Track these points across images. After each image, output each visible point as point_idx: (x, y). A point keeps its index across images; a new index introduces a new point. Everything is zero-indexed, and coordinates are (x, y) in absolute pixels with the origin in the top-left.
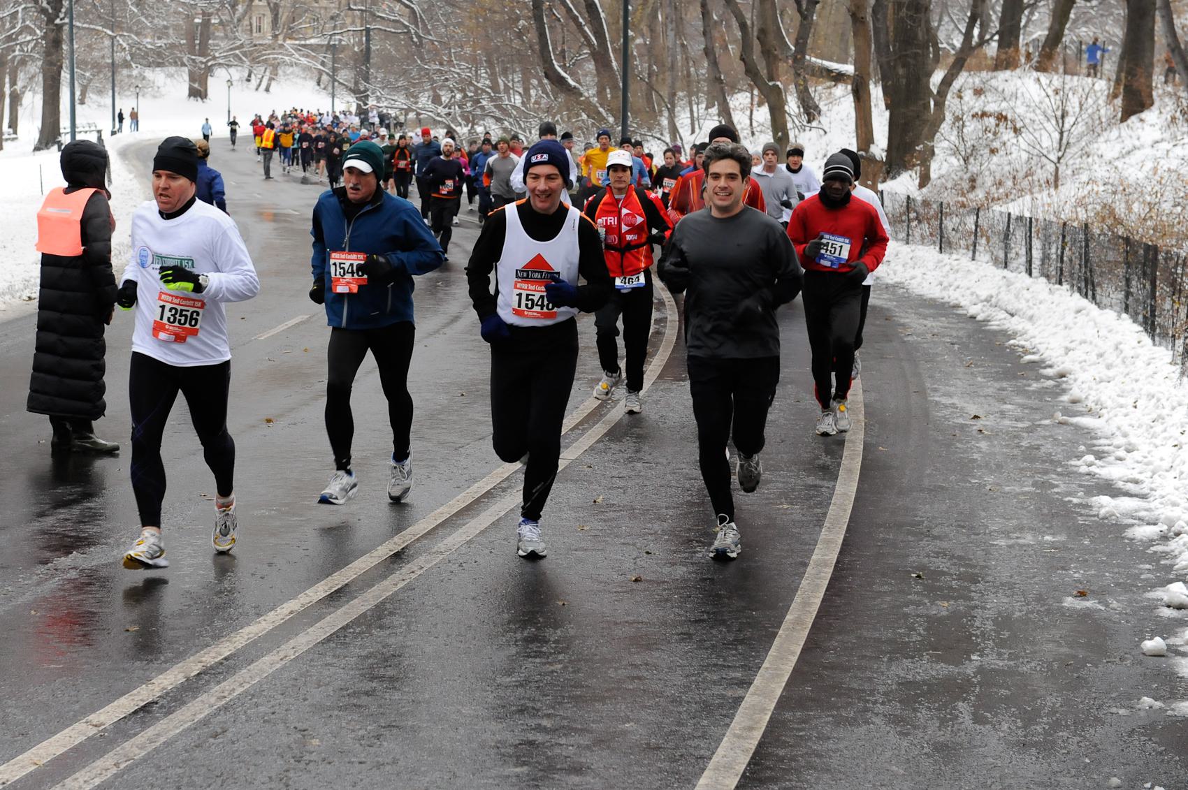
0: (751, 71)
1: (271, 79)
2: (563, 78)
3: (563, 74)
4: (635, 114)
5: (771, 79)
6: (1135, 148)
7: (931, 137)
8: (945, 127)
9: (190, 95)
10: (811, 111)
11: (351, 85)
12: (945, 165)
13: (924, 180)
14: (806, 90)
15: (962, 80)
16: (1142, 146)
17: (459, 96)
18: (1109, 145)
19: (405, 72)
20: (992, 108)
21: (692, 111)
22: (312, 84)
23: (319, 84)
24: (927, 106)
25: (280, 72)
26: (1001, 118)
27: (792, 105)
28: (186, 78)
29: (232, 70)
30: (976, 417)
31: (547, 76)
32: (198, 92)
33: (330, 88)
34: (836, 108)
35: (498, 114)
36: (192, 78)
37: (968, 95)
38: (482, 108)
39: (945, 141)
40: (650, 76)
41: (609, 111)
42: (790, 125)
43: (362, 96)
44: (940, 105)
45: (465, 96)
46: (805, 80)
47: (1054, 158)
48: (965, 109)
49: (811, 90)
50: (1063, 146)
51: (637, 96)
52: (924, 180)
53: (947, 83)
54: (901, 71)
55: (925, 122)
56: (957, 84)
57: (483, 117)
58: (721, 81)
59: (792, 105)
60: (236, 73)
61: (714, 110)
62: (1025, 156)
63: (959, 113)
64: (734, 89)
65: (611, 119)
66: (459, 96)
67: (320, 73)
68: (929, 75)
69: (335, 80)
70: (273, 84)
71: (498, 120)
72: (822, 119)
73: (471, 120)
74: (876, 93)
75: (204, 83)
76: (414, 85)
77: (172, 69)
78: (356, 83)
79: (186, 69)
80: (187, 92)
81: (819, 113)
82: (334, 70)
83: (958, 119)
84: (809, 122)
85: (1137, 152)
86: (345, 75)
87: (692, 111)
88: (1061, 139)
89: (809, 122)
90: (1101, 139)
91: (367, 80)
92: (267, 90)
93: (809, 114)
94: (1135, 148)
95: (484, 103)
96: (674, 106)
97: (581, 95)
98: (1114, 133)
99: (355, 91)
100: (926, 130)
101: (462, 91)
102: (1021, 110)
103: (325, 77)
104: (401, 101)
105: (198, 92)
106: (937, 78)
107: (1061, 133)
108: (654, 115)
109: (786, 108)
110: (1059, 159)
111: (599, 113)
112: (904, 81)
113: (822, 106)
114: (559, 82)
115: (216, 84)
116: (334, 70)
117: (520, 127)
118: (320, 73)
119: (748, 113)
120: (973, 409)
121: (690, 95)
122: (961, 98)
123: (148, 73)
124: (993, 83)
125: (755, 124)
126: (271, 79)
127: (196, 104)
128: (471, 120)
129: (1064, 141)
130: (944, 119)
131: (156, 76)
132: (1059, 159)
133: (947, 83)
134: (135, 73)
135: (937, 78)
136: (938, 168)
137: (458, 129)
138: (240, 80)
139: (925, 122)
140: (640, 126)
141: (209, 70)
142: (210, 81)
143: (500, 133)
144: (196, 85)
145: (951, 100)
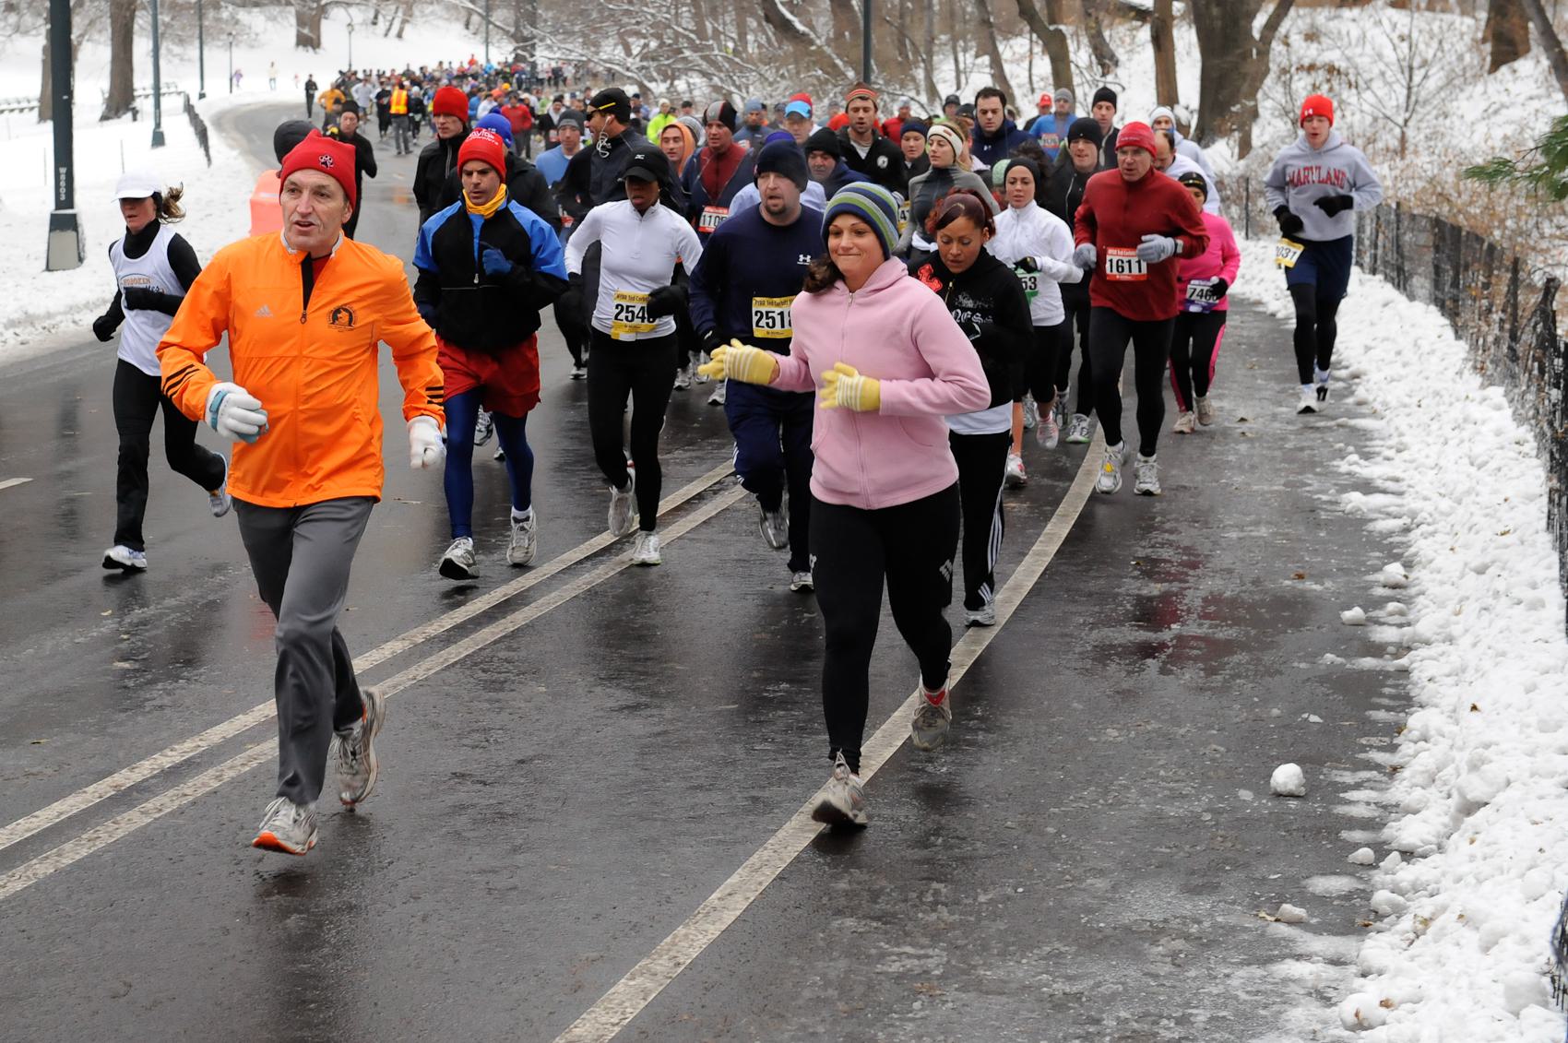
0: (1027, 13)
1: (404, 22)
2: (789, 22)
3: (789, 16)
4: (882, 67)
5: (1053, 21)
6: (1503, 106)
7: (1253, 95)
8: (1269, 81)
9: (298, 44)
10: (1105, 59)
11: (512, 30)
12: (1270, 129)
13: (1245, 147)
14: (1100, 34)
15: (1294, 23)
16: (1513, 104)
17: (653, 44)
18: (1470, 104)
19: (583, 13)
20: (1333, 56)
21: (956, 61)
22: (459, 26)
23: (467, 26)
24: (1246, 56)
25: (416, 12)
26: (1332, 69)
27: (1080, 55)
28: (293, 20)
29: (353, 11)
30: (1242, 420)
31: (768, 19)
32: (308, 40)
33: (483, 29)
34: (1136, 57)
35: (705, 66)
36: (301, 22)
37: (1296, 39)
38: (685, 59)
39: (1270, 99)
40: (902, 16)
41: (848, 63)
42: (1076, 80)
43: (525, 43)
44: (1264, 53)
45: (662, 44)
46: (1097, 21)
47: (1401, 121)
48: (1294, 59)
49: (1106, 34)
50: (1411, 103)
51: (883, 40)
52: (1245, 147)
53: (1272, 26)
54: (1215, 11)
55: (1244, 76)
56: (1282, 30)
57: (686, 71)
58: (990, 25)
59: (1080, 55)
60: (359, 15)
61: (986, 59)
62: (1369, 119)
63: (1285, 63)
64: (1010, 33)
65: (851, 74)
66: (653, 44)
67: (470, 12)
68: (1252, 16)
69: (489, 22)
70: (408, 27)
71: (704, 74)
72: (1119, 71)
73: (670, 76)
74: (1186, 39)
75: (316, 27)
76: (595, 30)
77: (275, 10)
78: (517, 27)
79: (292, 10)
80: (294, 40)
81: (1116, 64)
82: (489, 9)
83: (1284, 71)
84: (1104, 75)
85: (1504, 111)
86: (502, 16)
87: (956, 61)
88: (1409, 97)
89: (1104, 75)
90: (1462, 96)
91: (533, 25)
92: (399, 36)
93: (1103, 65)
94: (1503, 106)
95: (687, 53)
96: (930, 54)
97: (812, 42)
98: (1480, 88)
99: (517, 37)
100: (1245, 88)
101: (658, 36)
102: (1363, 62)
103: (475, 18)
104: (576, 51)
105: (308, 40)
106: (1259, 22)
107: (1409, 88)
108: (906, 66)
109: (1072, 56)
110: (1406, 121)
111: (835, 66)
112: (1218, 24)
113: (1121, 54)
114: (784, 27)
115: (333, 28)
116: (489, 9)
117: (734, 83)
118: (470, 12)
119: (1026, 65)
120: (1241, 413)
121: (954, 40)
122: (1287, 45)
123: (243, 15)
124: (1332, 24)
125: (1035, 79)
126: (404, 22)
127: (306, 55)
128: (670, 76)
129: (1413, 98)
130: (1268, 71)
131: (253, 19)
132: (1406, 121)
133: (1272, 26)
134: (225, 15)
135: (1259, 22)
136: (1259, 134)
137: (652, 86)
138: (364, 23)
139: (1244, 76)
140: (887, 83)
141: (323, 10)
142: (325, 26)
143: (707, 90)
144: (306, 31)
145: (1276, 47)
